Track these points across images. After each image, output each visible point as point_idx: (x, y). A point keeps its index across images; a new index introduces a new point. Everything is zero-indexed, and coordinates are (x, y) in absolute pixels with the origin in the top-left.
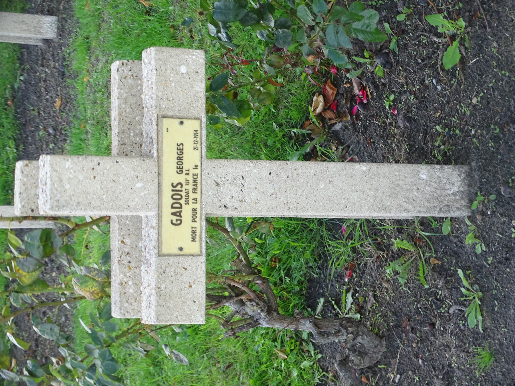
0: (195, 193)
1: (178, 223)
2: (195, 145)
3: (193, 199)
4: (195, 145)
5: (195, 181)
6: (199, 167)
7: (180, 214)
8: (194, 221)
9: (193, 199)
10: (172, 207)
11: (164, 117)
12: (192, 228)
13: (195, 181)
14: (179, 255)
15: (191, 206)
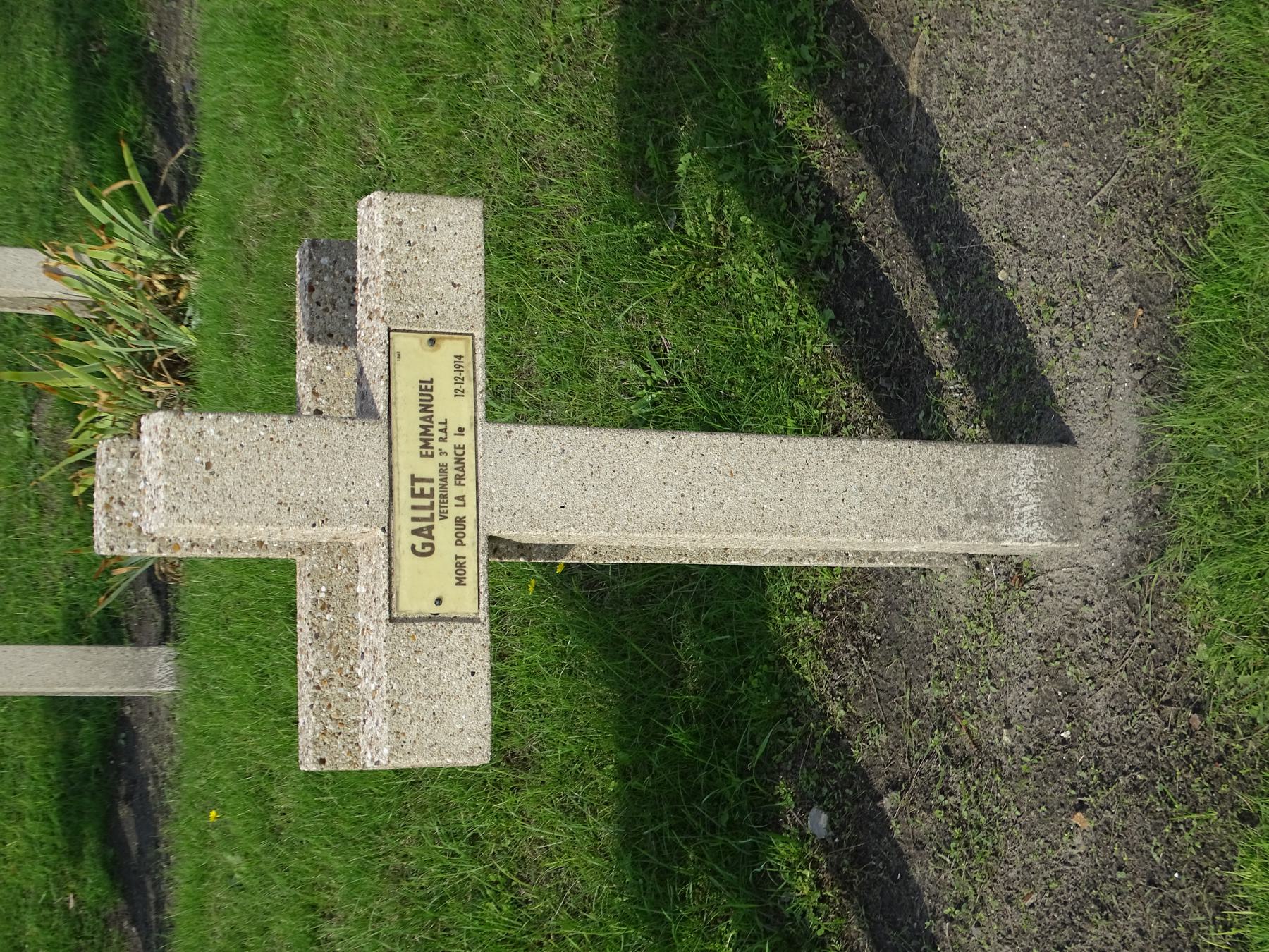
0: (460, 484)
1: (427, 551)
2: (458, 386)
3: (457, 498)
4: (458, 386)
5: (459, 460)
6: (469, 434)
7: (430, 533)
8: (459, 542)
9: (457, 498)
10: (414, 519)
11: (395, 330)
12: (457, 557)
13: (459, 460)
14: (434, 618)
15: (453, 512)
